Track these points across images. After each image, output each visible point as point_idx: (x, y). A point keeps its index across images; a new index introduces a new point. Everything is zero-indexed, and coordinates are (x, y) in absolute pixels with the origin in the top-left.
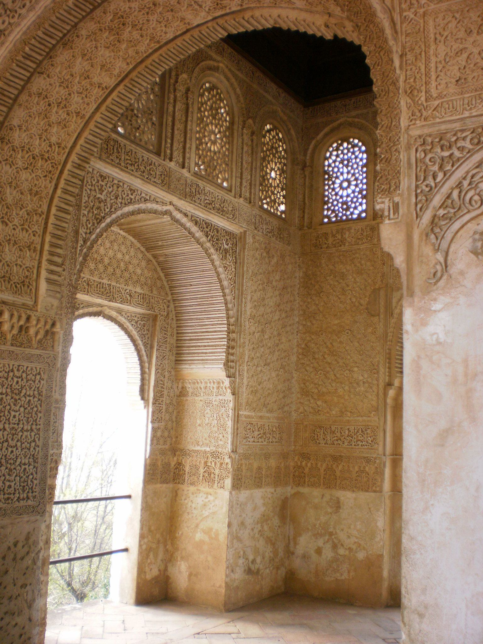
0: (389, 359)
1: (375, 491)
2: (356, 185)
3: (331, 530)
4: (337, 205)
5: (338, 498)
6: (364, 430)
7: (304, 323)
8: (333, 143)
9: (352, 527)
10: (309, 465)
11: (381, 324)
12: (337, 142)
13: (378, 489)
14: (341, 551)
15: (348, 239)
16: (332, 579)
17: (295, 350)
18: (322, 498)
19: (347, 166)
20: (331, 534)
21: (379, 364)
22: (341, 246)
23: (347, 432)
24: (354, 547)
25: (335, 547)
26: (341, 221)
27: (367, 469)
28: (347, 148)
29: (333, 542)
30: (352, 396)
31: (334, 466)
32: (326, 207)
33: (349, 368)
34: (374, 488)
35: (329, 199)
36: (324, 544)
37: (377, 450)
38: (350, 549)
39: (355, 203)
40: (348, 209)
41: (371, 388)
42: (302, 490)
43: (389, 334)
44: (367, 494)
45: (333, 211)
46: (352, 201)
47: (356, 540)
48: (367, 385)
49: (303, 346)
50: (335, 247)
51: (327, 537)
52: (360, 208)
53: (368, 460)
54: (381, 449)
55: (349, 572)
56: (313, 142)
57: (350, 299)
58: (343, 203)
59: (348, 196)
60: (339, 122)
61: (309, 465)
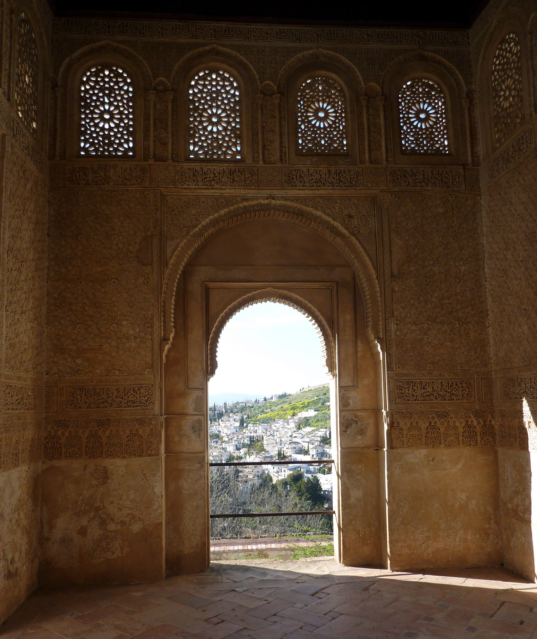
0: (164, 312)
1: (149, 455)
2: (121, 120)
3: (98, 505)
4: (97, 138)
5: (105, 467)
6: (136, 389)
7: (56, 268)
8: (92, 68)
9: (124, 497)
10: (67, 434)
11: (154, 275)
12: (96, 66)
13: (153, 452)
14: (112, 527)
15: (113, 178)
16: (101, 560)
17: (46, 300)
18: (85, 470)
19: (109, 96)
20: (98, 509)
21: (153, 317)
22: (103, 184)
23: (115, 393)
24: (127, 520)
25: (103, 523)
26: (103, 156)
27: (141, 432)
28: (108, 76)
29: (101, 517)
30: (121, 353)
31: (100, 433)
32: (83, 138)
33: (116, 321)
34: (149, 452)
35: (86, 129)
36: (89, 522)
37: (153, 409)
38: (123, 523)
39: (119, 139)
40: (111, 144)
41: (145, 343)
42: (56, 463)
43: (164, 285)
44: (141, 458)
45: (92, 144)
46: (115, 136)
47: (129, 512)
48: (138, 340)
49: (56, 295)
50: (97, 184)
51: (92, 514)
52: (126, 146)
53: (141, 422)
54: (157, 408)
55: (122, 549)
56: (67, 60)
57: (117, 245)
58: (104, 137)
59: (111, 129)
60: (100, 43)
61: (67, 434)
